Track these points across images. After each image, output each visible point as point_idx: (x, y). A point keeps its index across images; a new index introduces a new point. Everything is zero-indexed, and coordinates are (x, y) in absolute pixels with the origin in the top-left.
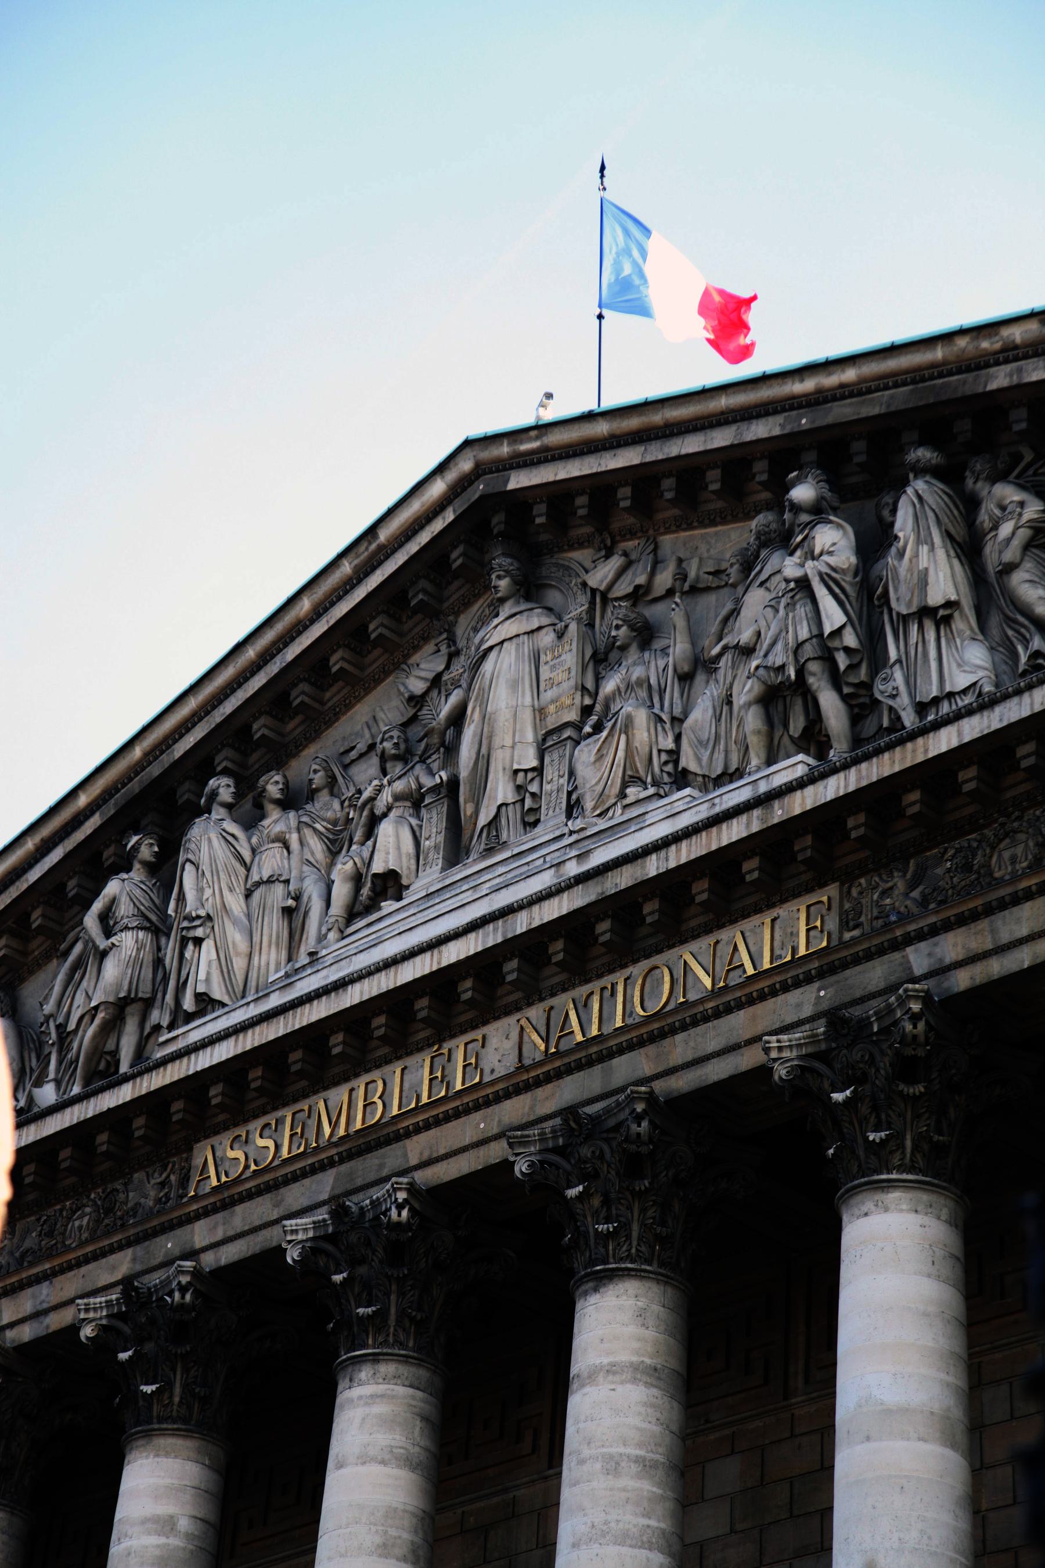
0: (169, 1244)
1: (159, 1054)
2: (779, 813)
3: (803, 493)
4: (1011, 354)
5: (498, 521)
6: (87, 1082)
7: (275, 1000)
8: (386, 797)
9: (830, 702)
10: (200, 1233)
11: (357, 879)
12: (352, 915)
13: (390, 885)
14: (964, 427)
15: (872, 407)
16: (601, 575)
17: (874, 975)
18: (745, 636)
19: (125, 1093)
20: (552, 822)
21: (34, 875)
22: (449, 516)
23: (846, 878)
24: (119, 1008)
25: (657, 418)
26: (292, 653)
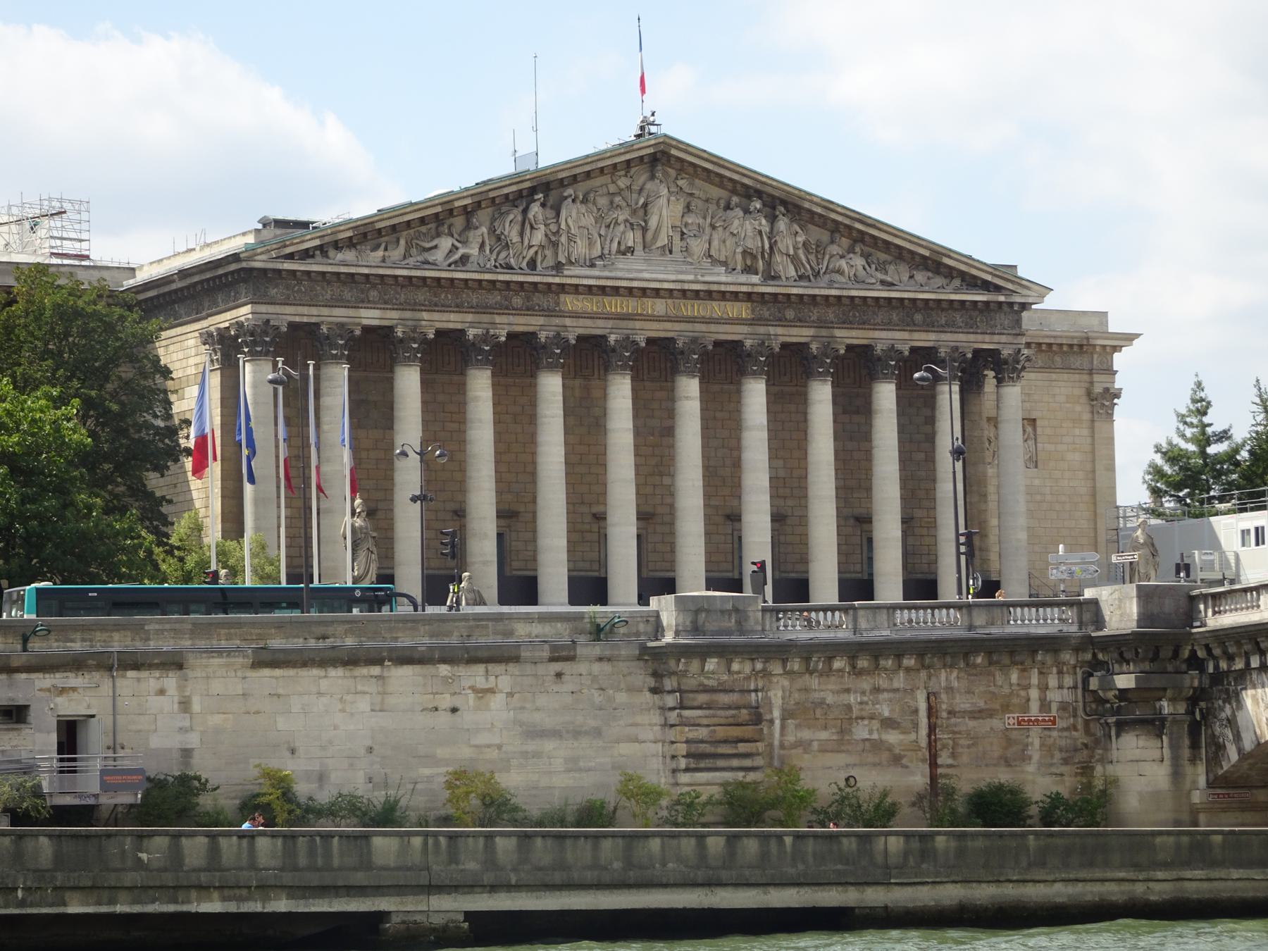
0: (557, 321)
1: (566, 273)
2: (757, 289)
4: (811, 201)
5: (659, 156)
8: (621, 218)
9: (760, 262)
10: (568, 322)
12: (619, 252)
13: (631, 250)
14: (790, 207)
15: (776, 193)
16: (680, 183)
17: (762, 330)
19: (557, 280)
20: (677, 255)
21: (506, 191)
22: (651, 150)
23: (753, 302)
24: (542, 247)
26: (601, 164)
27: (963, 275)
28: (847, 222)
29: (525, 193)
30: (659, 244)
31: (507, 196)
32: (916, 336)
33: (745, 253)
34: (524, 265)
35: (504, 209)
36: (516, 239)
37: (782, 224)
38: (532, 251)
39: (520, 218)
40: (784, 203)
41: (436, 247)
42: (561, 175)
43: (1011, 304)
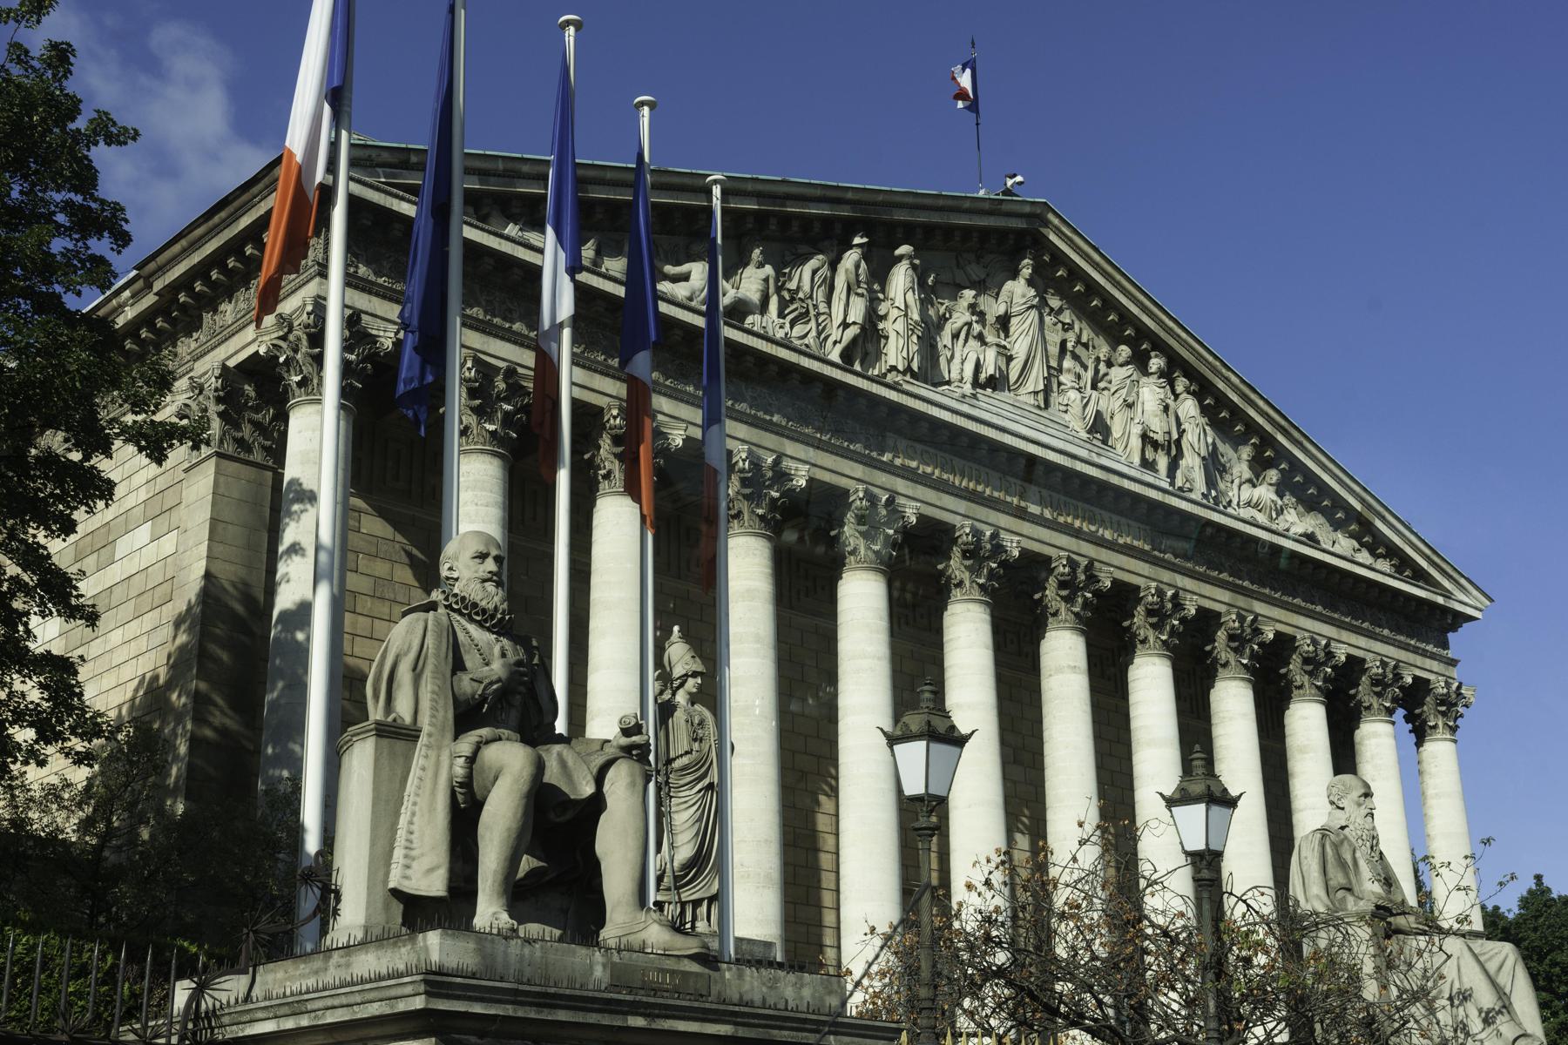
3: (1156, 363)
6: (842, 355)
7: (965, 408)
10: (901, 485)
11: (978, 367)
18: (1130, 400)
25: (1118, 277)
27: (1392, 552)
28: (1268, 428)
29: (838, 229)
30: (1030, 387)
31: (807, 220)
32: (1346, 636)
33: (1145, 437)
34: (835, 356)
35: (803, 249)
36: (822, 308)
37: (1188, 408)
38: (852, 332)
39: (825, 271)
40: (1190, 373)
41: (685, 277)
42: (900, 216)
43: (1445, 610)
